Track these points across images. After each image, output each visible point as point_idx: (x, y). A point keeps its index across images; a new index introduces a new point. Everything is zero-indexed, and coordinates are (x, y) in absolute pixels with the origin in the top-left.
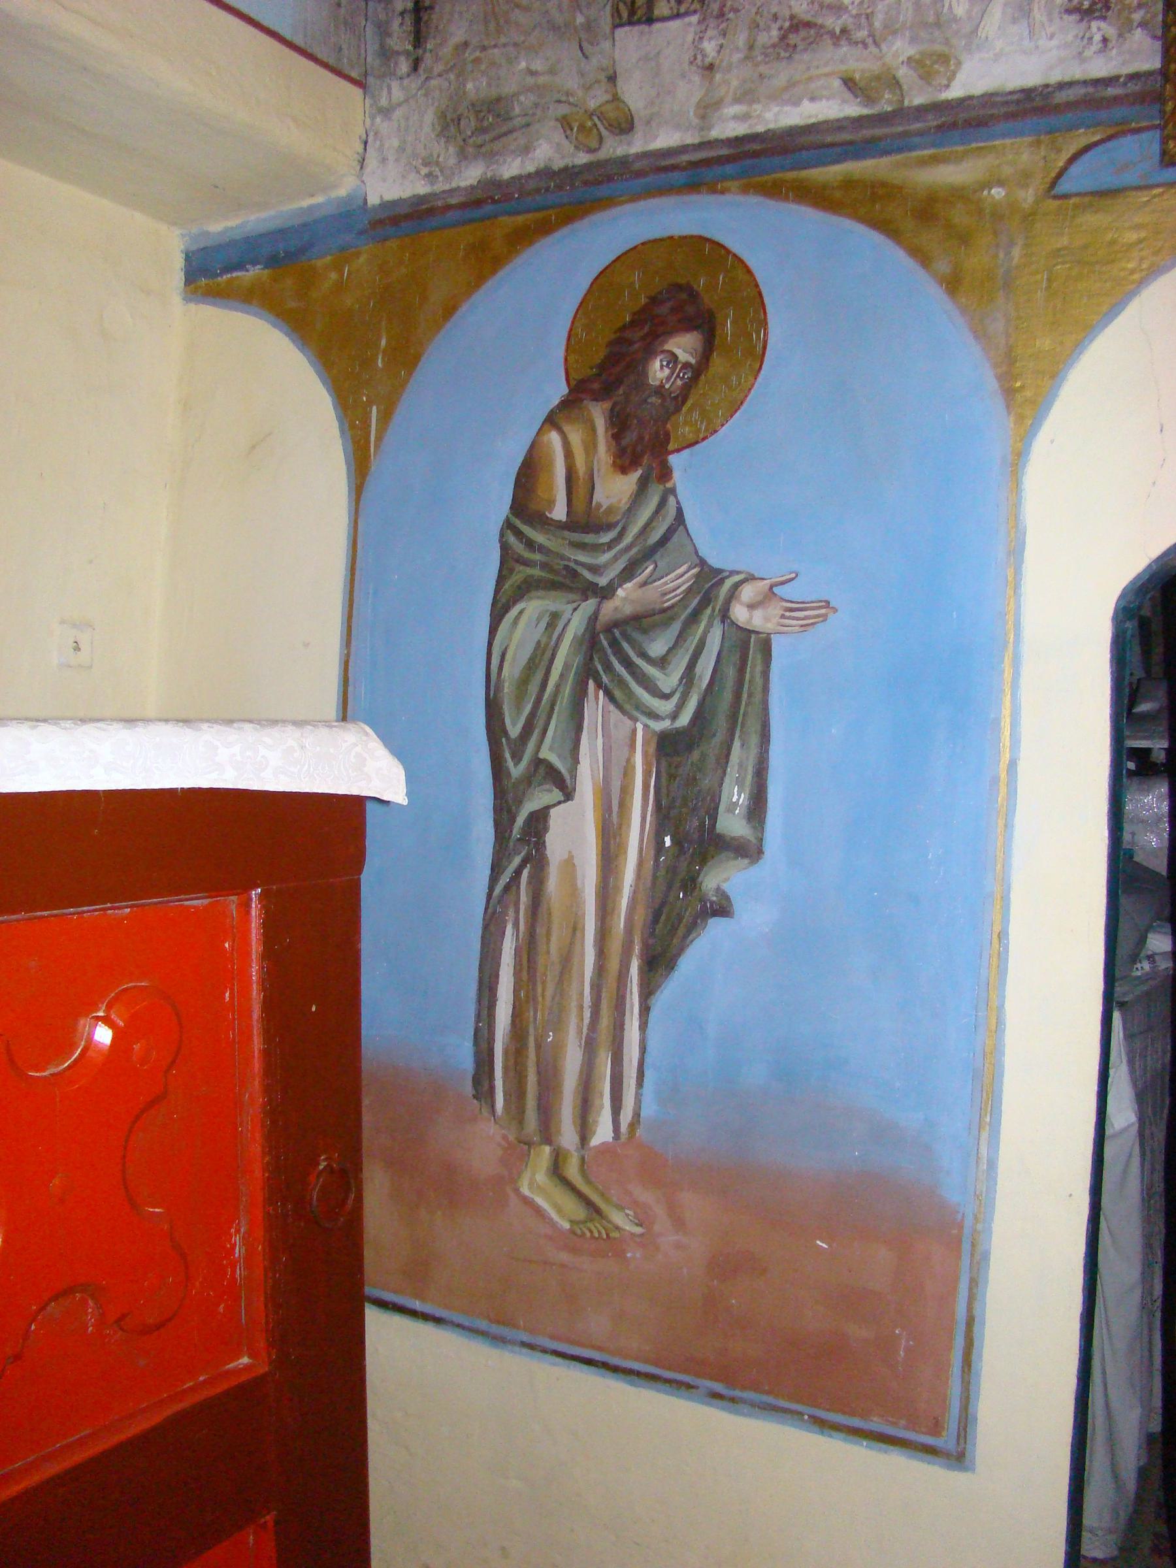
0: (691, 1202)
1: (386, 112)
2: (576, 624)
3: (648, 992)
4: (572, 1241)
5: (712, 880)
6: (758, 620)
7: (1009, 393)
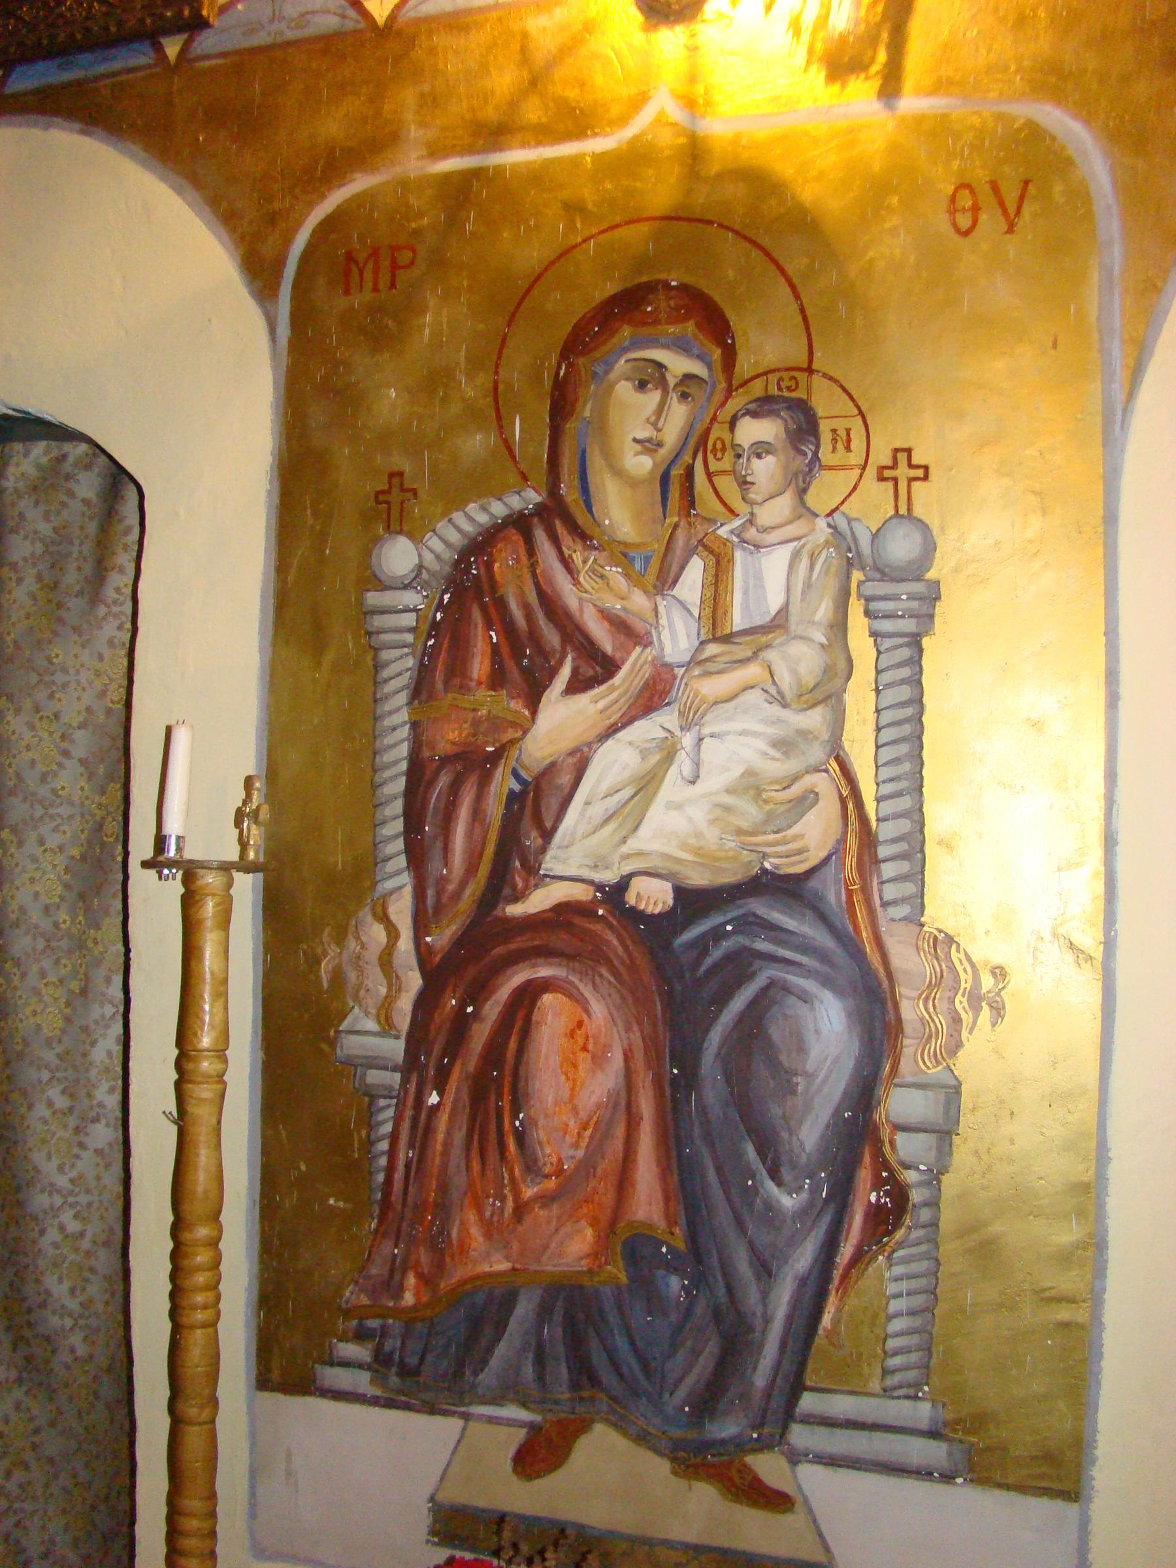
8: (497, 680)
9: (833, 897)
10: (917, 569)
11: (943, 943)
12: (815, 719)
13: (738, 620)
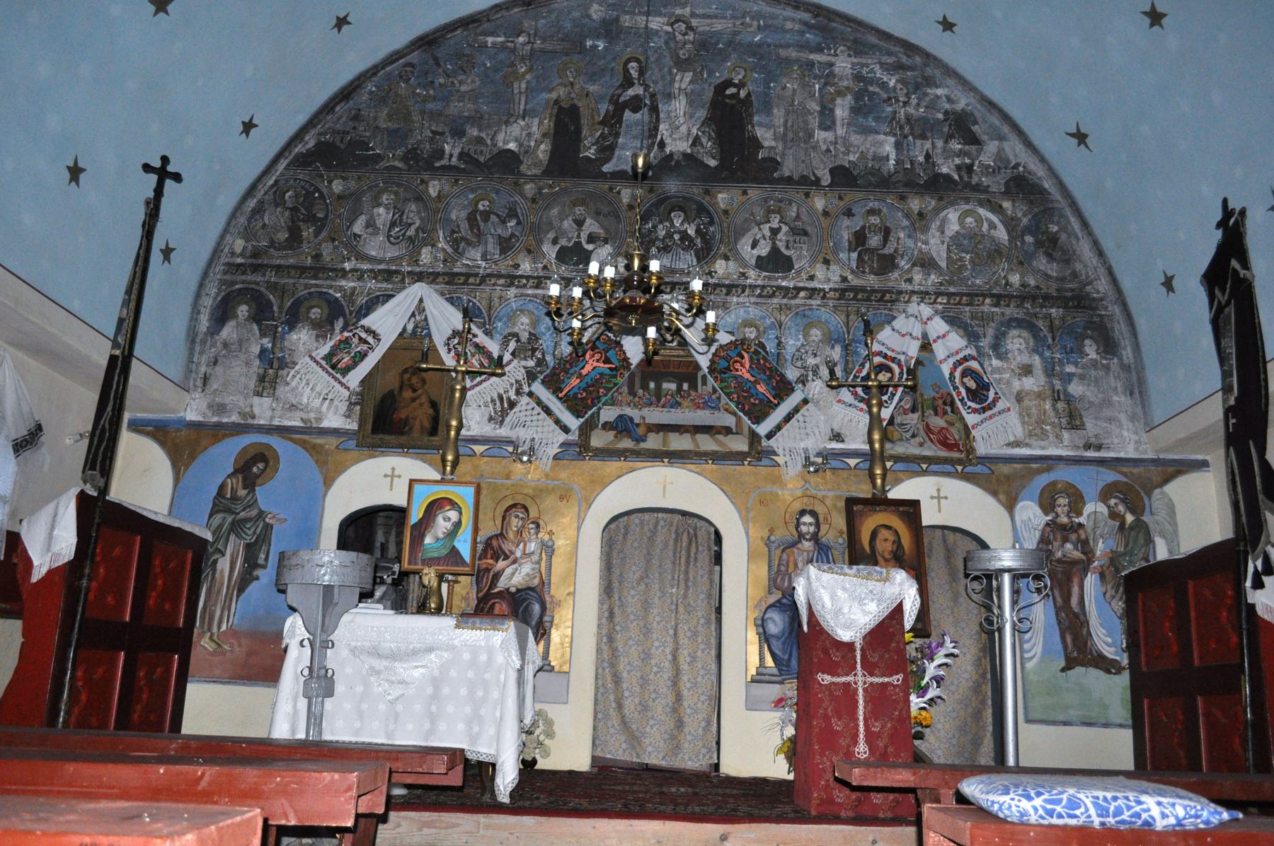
0: (244, 641)
1: (194, 399)
2: (230, 519)
3: (238, 596)
4: (211, 654)
5: (255, 573)
6: (271, 522)
7: (325, 483)
8: (492, 558)
9: (538, 590)
10: (552, 547)
11: (552, 597)
12: (537, 566)
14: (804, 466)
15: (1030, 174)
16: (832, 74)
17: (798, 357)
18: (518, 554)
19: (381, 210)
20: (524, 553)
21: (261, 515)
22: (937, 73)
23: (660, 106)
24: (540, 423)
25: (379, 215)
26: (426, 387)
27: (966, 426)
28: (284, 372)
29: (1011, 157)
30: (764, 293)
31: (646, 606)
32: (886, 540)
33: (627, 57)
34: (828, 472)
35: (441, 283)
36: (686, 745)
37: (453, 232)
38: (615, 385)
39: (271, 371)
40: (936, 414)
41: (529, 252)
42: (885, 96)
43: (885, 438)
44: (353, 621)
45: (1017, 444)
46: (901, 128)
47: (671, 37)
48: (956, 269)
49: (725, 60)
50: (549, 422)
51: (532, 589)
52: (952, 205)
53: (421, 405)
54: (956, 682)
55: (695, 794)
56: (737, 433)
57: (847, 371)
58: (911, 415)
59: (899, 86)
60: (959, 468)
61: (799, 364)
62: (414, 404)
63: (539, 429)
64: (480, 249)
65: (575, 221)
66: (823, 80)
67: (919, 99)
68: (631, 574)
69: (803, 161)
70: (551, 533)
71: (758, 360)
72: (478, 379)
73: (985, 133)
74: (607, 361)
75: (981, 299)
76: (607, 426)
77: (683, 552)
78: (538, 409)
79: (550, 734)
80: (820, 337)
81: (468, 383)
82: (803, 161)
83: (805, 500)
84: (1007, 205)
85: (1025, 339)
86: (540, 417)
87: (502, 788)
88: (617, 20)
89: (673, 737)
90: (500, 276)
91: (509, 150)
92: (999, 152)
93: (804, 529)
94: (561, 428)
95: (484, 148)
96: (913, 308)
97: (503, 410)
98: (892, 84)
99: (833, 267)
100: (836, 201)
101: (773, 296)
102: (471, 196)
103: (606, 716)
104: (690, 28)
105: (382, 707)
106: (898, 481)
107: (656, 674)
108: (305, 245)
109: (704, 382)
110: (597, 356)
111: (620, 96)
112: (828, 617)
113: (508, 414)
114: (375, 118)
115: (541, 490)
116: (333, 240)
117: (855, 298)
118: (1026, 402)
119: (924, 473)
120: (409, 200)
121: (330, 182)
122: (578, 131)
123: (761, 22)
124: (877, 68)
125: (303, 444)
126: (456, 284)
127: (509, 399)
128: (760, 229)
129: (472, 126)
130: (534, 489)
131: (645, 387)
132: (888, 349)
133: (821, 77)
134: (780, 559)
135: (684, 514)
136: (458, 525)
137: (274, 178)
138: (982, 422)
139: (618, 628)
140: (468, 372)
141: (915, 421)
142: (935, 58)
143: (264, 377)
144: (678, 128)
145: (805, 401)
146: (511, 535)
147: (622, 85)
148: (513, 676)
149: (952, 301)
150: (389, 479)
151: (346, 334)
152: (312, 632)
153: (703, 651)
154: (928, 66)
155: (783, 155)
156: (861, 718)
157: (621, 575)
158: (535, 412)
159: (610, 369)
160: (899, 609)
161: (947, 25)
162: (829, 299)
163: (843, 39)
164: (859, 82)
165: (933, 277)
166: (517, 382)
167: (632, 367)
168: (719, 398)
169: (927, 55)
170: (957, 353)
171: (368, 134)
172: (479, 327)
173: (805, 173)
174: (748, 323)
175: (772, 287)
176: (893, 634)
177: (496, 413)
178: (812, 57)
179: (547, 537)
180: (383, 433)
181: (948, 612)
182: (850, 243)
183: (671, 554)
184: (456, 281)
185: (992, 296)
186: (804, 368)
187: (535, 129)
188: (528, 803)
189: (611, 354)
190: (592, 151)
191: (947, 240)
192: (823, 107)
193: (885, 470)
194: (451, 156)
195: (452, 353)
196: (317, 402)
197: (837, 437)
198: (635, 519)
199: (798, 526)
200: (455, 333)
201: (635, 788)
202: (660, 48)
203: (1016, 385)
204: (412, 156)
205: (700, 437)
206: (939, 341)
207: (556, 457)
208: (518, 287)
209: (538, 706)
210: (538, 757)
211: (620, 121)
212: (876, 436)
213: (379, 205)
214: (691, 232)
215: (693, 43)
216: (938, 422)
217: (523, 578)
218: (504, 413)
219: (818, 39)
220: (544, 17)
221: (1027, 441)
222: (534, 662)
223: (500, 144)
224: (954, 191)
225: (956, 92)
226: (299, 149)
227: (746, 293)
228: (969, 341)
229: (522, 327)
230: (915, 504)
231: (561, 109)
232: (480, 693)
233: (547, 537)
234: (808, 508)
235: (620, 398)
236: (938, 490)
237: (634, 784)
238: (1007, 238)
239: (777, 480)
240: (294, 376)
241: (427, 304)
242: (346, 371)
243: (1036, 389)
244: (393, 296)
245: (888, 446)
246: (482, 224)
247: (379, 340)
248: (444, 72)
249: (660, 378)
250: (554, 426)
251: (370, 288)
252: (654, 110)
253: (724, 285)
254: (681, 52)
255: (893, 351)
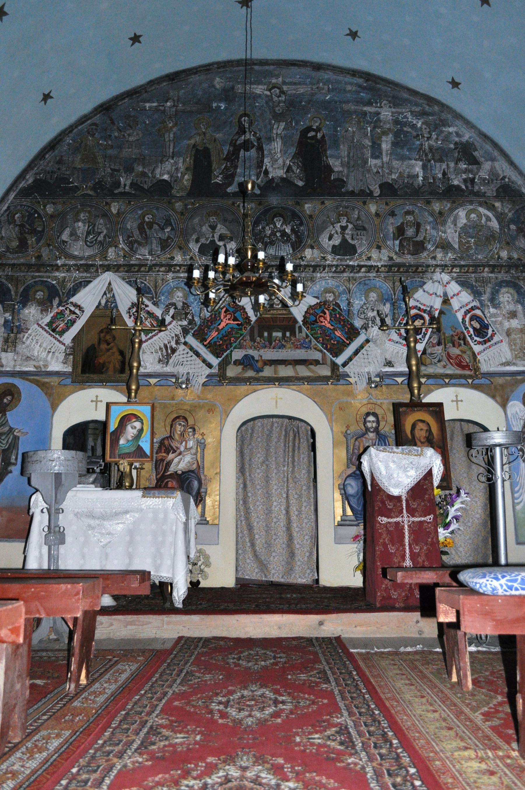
5: (9, 469)
6: (18, 434)
7: (52, 408)
9: (196, 472)
10: (204, 443)
11: (205, 476)
13: (188, 447)
14: (368, 384)
15: (513, 183)
16: (379, 120)
17: (362, 312)
18: (182, 449)
19: (80, 224)
20: (186, 448)
21: (11, 430)
22: (450, 116)
23: (264, 146)
24: (192, 362)
25: (79, 227)
26: (116, 341)
27: (474, 353)
28: (21, 335)
29: (500, 172)
30: (338, 270)
31: (267, 479)
32: (422, 429)
33: (241, 113)
34: (384, 387)
35: (123, 271)
36: (297, 568)
37: (129, 237)
38: (241, 335)
39: (12, 335)
40: (454, 346)
41: (180, 248)
42: (415, 134)
43: (420, 362)
44: (75, 496)
45: (508, 364)
46: (426, 155)
47: (270, 99)
48: (465, 248)
49: (306, 113)
50: (199, 361)
51: (193, 471)
52: (461, 206)
53: (113, 353)
54: (471, 521)
55: (303, 598)
56: (323, 364)
57: (394, 320)
58: (437, 347)
59: (424, 127)
60: (470, 381)
61: (363, 316)
62: (108, 353)
63: (193, 366)
64: (147, 248)
65: (210, 226)
66: (373, 125)
67: (438, 135)
68: (257, 459)
69: (361, 180)
70: (203, 434)
71: (336, 315)
72: (150, 335)
73: (482, 157)
74: (235, 319)
75: (482, 268)
76: (237, 363)
77: (291, 443)
78: (191, 353)
79: (208, 564)
80: (376, 298)
81: (144, 338)
82: (361, 180)
83: (369, 406)
84: (498, 204)
85: (511, 294)
86: (192, 358)
87: (177, 598)
88: (233, 88)
89: (288, 563)
90: (161, 265)
91: (164, 180)
92: (491, 169)
93: (369, 425)
94: (206, 365)
95: (147, 180)
96: (437, 276)
97: (168, 355)
98: (419, 125)
99: (383, 251)
100: (384, 206)
101: (344, 271)
102: (140, 212)
103: (244, 551)
104: (282, 92)
105: (97, 550)
106: (429, 392)
107: (275, 523)
108: (30, 250)
109: (300, 331)
110: (229, 316)
111: (236, 140)
112: (384, 480)
113: (171, 357)
114: (73, 162)
115: (196, 407)
116: (49, 245)
117: (398, 271)
118: (513, 336)
119: (447, 385)
120: (98, 216)
121: (45, 206)
122: (210, 165)
123: (330, 86)
124: (409, 115)
125: (37, 383)
126: (133, 272)
127: (171, 347)
128: (334, 227)
129: (139, 165)
130: (191, 406)
131: (261, 336)
132: (421, 304)
133: (371, 123)
134: (354, 445)
135: (290, 418)
136: (141, 431)
137: (7, 205)
138: (484, 350)
139: (250, 494)
140: (142, 330)
141: (440, 352)
142: (448, 107)
143: (8, 339)
144: (277, 160)
145: (367, 341)
146: (177, 437)
147: (237, 133)
148: (181, 527)
149: (463, 271)
150: (94, 403)
151: (61, 308)
152: (49, 503)
153: (306, 507)
154: (443, 112)
155: (348, 176)
156: (407, 544)
157: (250, 460)
158: (189, 355)
159: (238, 324)
160: (429, 474)
161: (455, 84)
162: (381, 272)
163: (386, 96)
164: (397, 124)
165: (450, 255)
166: (176, 335)
167: (252, 323)
168: (310, 341)
169: (442, 105)
170: (467, 305)
171: (68, 173)
172: (148, 300)
173: (362, 188)
174: (327, 291)
175: (343, 265)
176: (426, 490)
177: (163, 357)
178: (365, 109)
179: (200, 437)
180: (89, 373)
181: (465, 475)
182: (394, 234)
183: (282, 445)
184: (133, 270)
185: (489, 266)
186: (366, 319)
187: (180, 165)
188: (194, 608)
189: (238, 314)
190: (220, 178)
191: (459, 229)
192: (374, 143)
193: (420, 384)
194: (125, 185)
195: (132, 318)
196: (44, 355)
197: (389, 364)
198: (258, 423)
199: (365, 423)
200: (133, 305)
201: (264, 596)
202: (262, 106)
203: (506, 325)
204: (99, 186)
205: (299, 368)
206: (455, 297)
207: (204, 385)
208: (174, 272)
209: (199, 547)
210: (200, 579)
211: (238, 158)
212: (414, 362)
213: (79, 221)
214: (288, 230)
215: (284, 102)
216: (455, 351)
217: (186, 465)
218: (168, 357)
219: (369, 96)
220: (183, 89)
221: (514, 361)
222: (195, 518)
223: (158, 176)
224: (462, 196)
225: (462, 129)
226: (22, 184)
227: (326, 271)
228: (475, 297)
229: (178, 299)
230: (440, 405)
231: (197, 150)
232: (160, 539)
233: (200, 437)
234: (372, 411)
235: (245, 344)
236: (457, 396)
237: (264, 593)
238: (498, 227)
239: (351, 394)
240: (28, 338)
241: (114, 286)
242: (62, 333)
243: (519, 327)
244: (91, 282)
245: (423, 368)
246: (147, 230)
247: (83, 311)
248: (118, 128)
249: (270, 329)
250: (202, 364)
251: (75, 277)
252: (260, 149)
253: (311, 266)
254: (277, 109)
255: (424, 305)
